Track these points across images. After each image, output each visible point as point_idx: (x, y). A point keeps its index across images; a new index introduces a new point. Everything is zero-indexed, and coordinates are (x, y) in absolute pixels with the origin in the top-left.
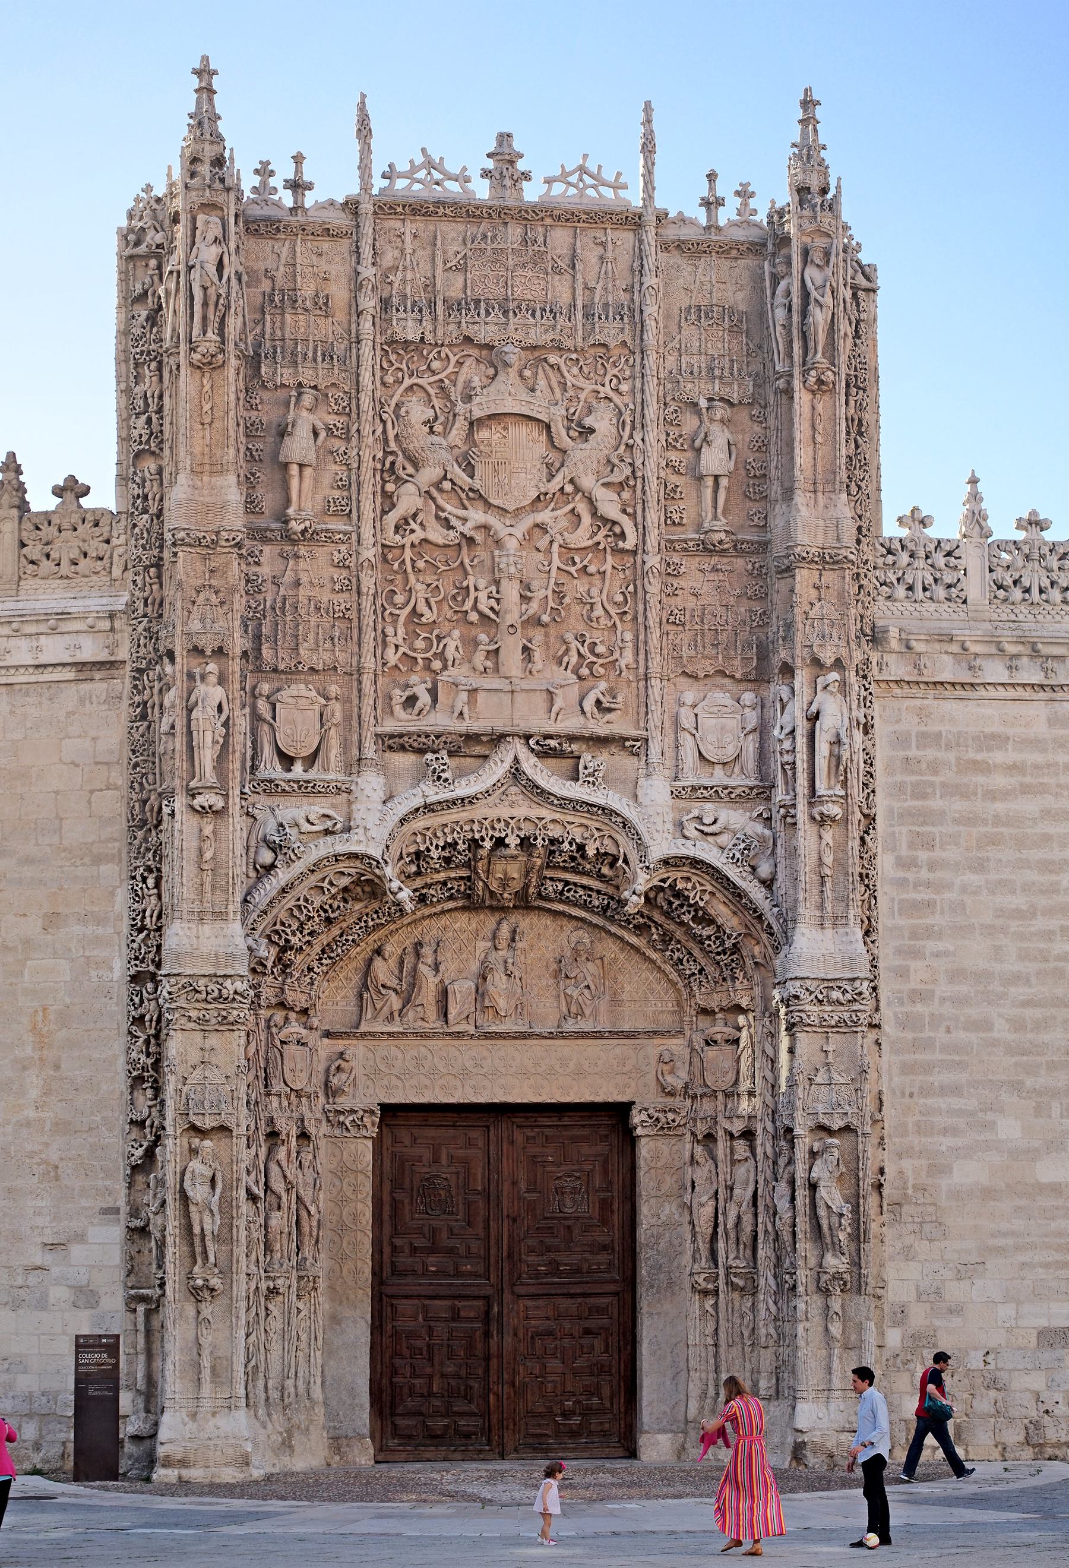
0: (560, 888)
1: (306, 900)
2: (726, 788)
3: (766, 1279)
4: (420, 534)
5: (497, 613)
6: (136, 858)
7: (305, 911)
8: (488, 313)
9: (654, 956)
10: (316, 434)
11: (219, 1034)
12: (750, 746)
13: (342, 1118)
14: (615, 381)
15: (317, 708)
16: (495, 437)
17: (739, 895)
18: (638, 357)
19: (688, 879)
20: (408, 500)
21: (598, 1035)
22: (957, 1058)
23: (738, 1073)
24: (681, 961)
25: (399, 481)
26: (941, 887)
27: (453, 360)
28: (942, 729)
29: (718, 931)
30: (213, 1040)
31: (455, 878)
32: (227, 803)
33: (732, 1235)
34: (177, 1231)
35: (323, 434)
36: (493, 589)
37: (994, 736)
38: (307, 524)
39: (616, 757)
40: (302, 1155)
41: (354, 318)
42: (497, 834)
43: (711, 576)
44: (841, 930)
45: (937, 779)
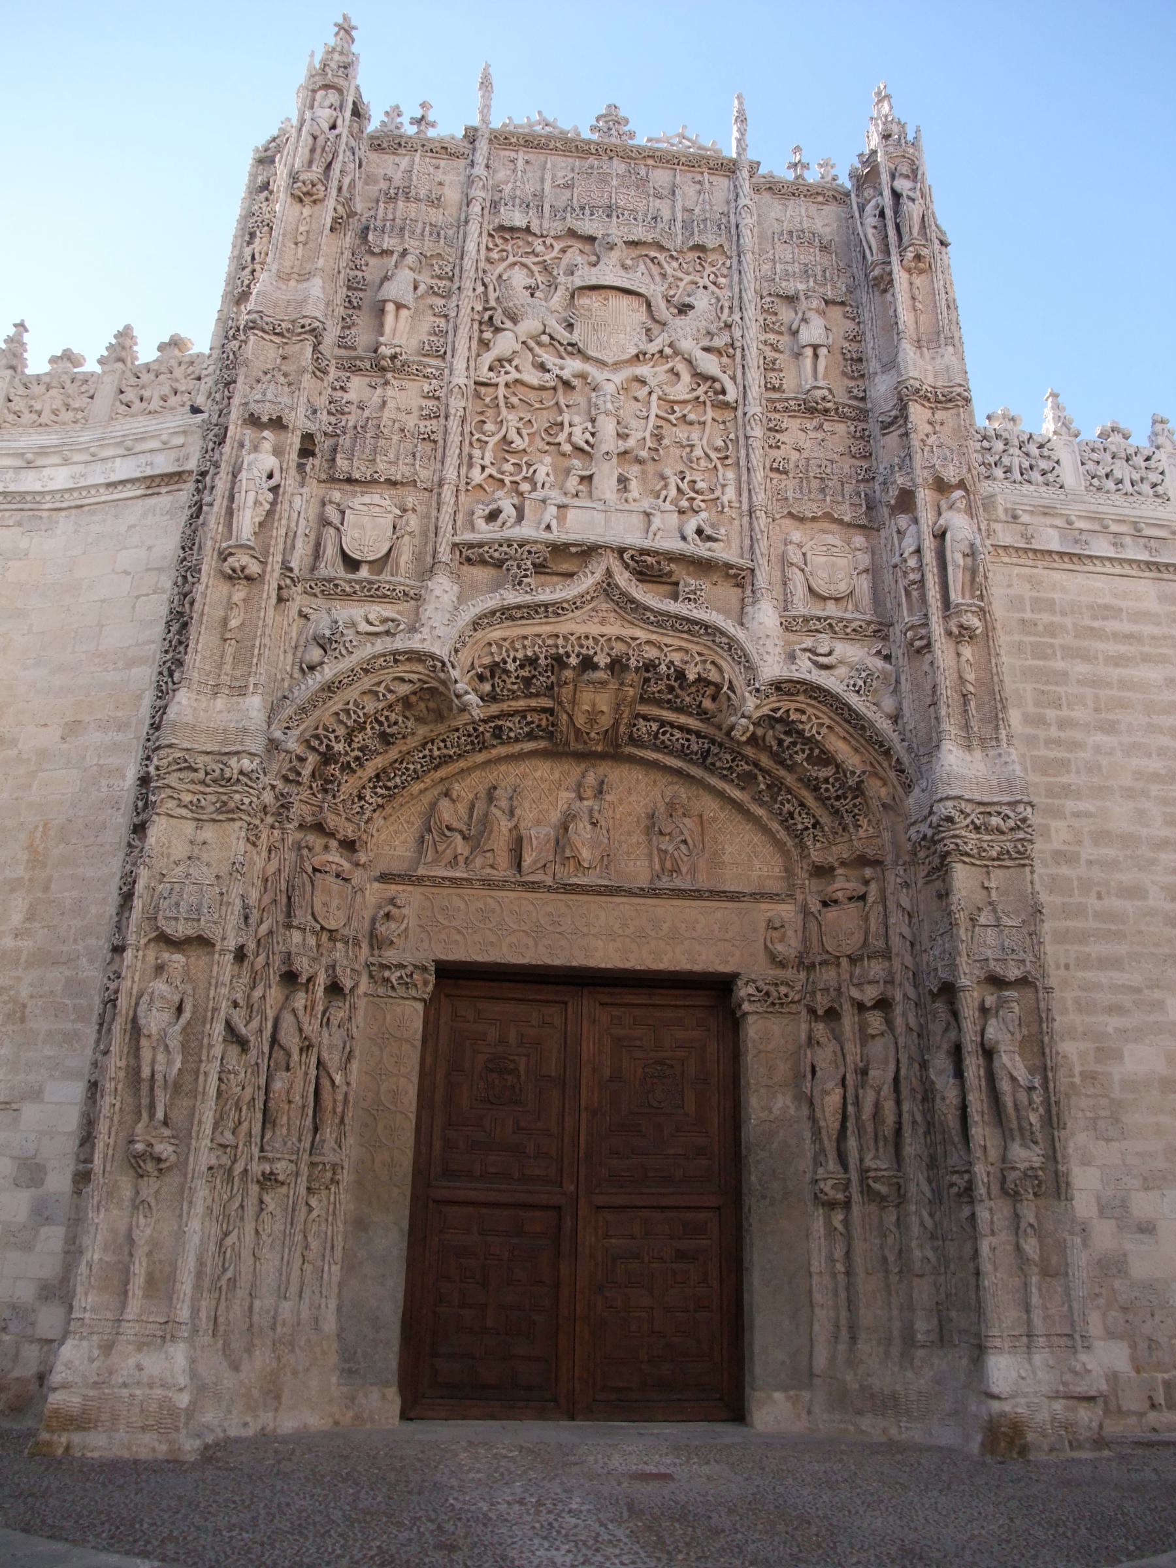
0: (655, 728)
1: (356, 704)
2: (841, 620)
3: (918, 1183)
4: (514, 375)
5: (592, 447)
6: (166, 652)
7: (354, 717)
8: (592, 215)
9: (760, 812)
10: (416, 288)
11: (216, 826)
12: (864, 584)
13: (387, 974)
14: (712, 276)
15: (391, 517)
16: (596, 305)
17: (863, 728)
18: (735, 260)
19: (803, 712)
20: (504, 344)
21: (695, 894)
22: (1113, 927)
23: (867, 933)
24: (791, 815)
25: (497, 330)
26: (1074, 745)
27: (557, 247)
28: (1055, 596)
29: (837, 772)
30: (208, 833)
31: (534, 710)
32: (264, 571)
33: (870, 1128)
34: (122, 1074)
35: (422, 288)
36: (589, 425)
37: (1106, 607)
38: (398, 350)
39: (719, 588)
40: (332, 1010)
41: (464, 208)
42: (584, 651)
43: (812, 435)
44: (992, 753)
45: (1057, 642)
